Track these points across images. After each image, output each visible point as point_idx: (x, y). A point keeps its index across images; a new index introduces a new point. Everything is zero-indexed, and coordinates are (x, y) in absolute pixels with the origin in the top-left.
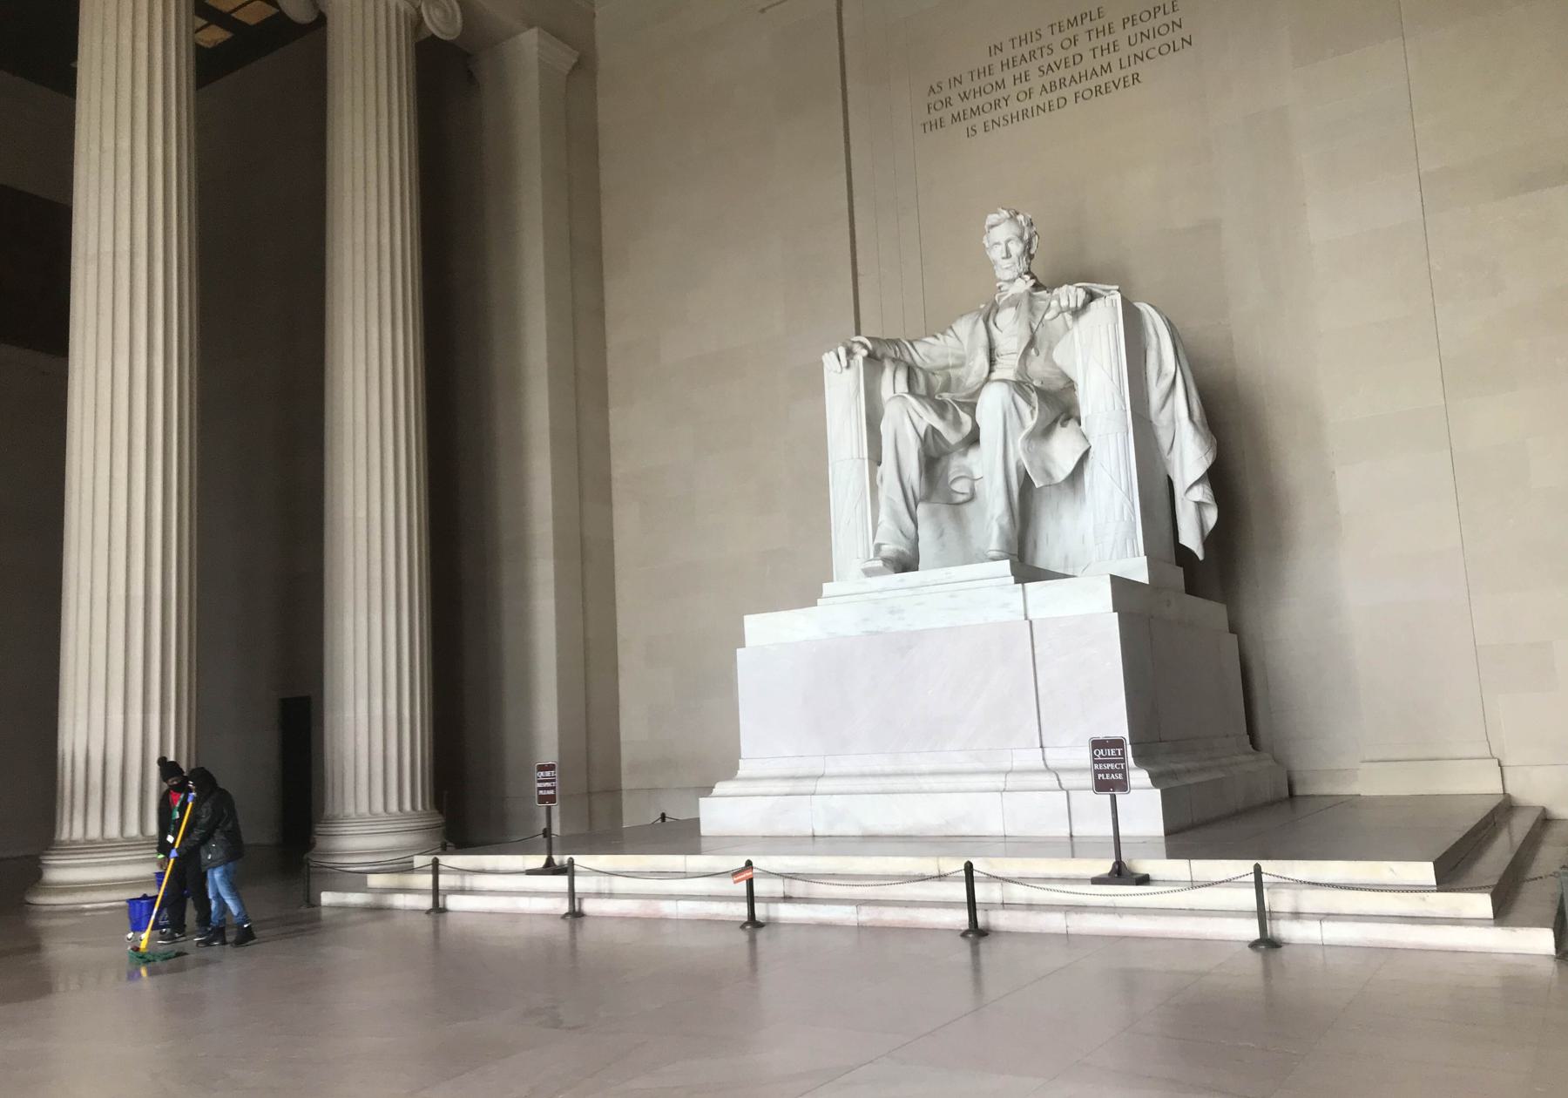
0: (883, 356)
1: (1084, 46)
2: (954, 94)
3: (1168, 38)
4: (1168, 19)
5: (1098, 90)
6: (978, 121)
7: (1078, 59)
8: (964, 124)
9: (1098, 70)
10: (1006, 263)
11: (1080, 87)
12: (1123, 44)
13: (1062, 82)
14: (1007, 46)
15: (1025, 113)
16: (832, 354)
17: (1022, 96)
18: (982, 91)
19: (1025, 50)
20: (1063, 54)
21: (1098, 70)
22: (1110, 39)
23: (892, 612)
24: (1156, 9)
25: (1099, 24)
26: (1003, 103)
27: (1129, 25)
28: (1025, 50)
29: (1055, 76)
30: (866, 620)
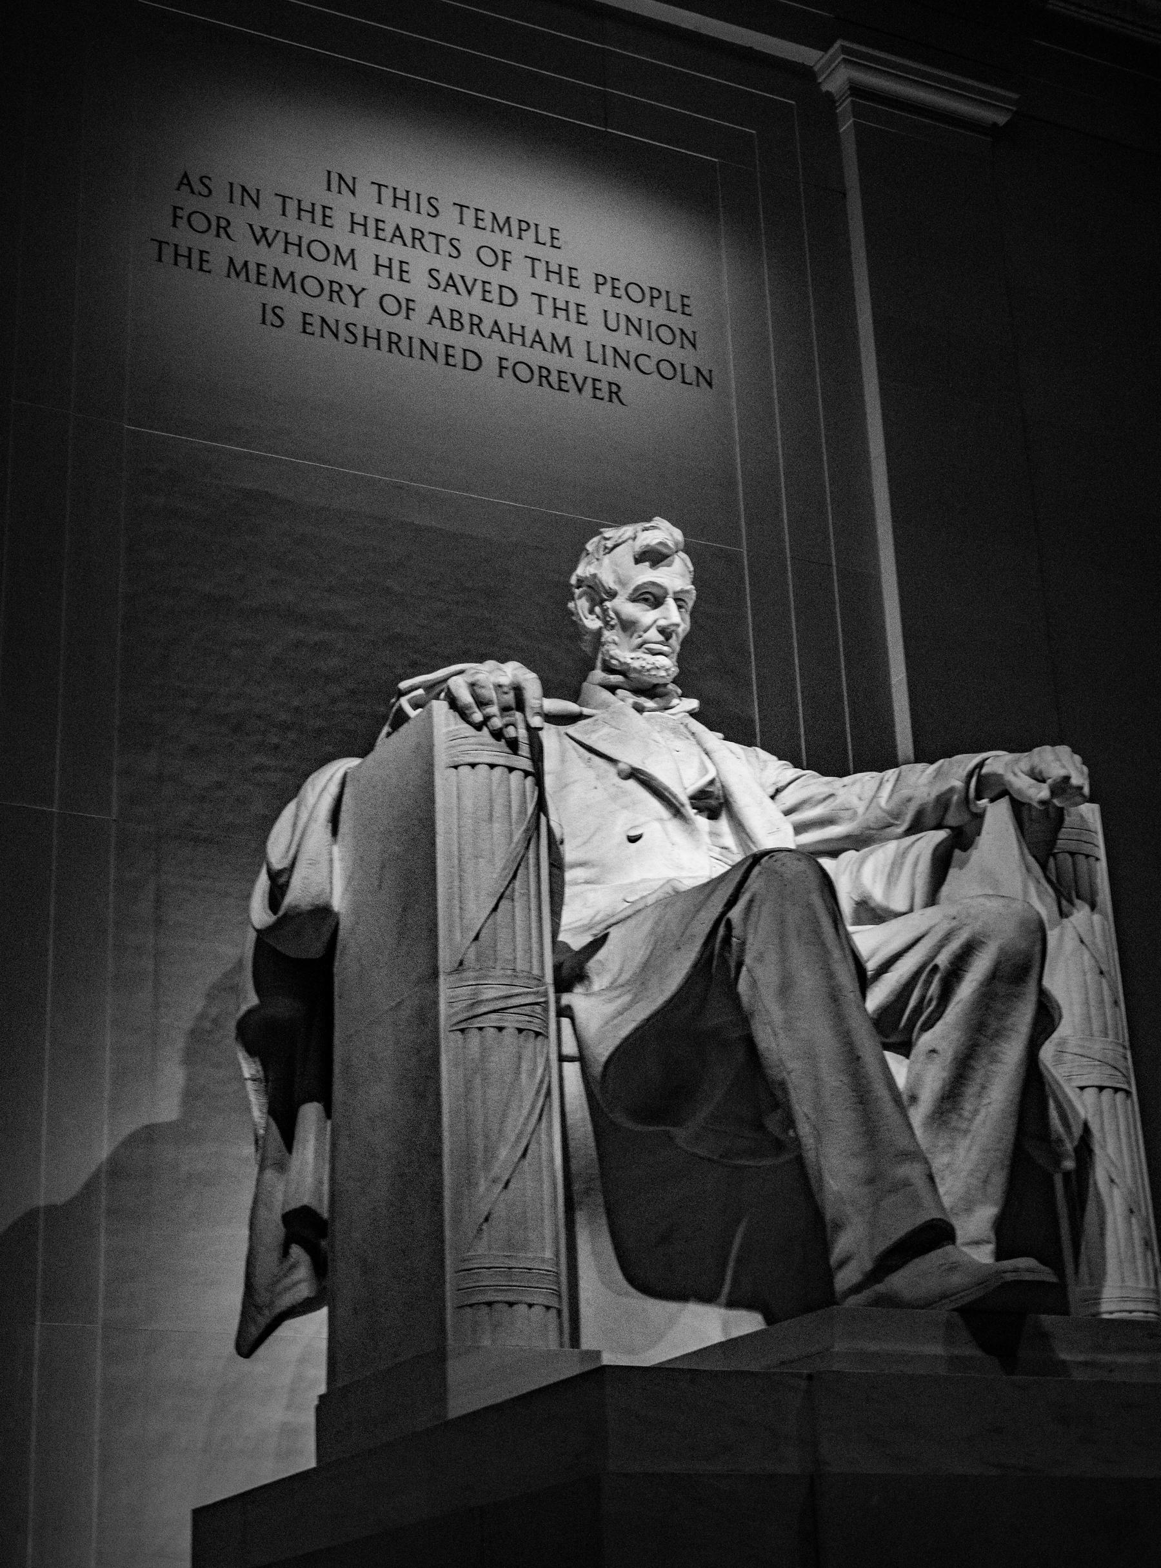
3: (675, 353)
4: (677, 321)
6: (294, 304)
7: (508, 297)
8: (254, 295)
9: (547, 341)
12: (593, 315)
13: (476, 324)
14: (365, 191)
18: (301, 247)
19: (408, 220)
20: (483, 273)
21: (547, 341)
22: (574, 297)
24: (655, 294)
25: (555, 258)
26: (346, 294)
27: (606, 290)
28: (408, 220)
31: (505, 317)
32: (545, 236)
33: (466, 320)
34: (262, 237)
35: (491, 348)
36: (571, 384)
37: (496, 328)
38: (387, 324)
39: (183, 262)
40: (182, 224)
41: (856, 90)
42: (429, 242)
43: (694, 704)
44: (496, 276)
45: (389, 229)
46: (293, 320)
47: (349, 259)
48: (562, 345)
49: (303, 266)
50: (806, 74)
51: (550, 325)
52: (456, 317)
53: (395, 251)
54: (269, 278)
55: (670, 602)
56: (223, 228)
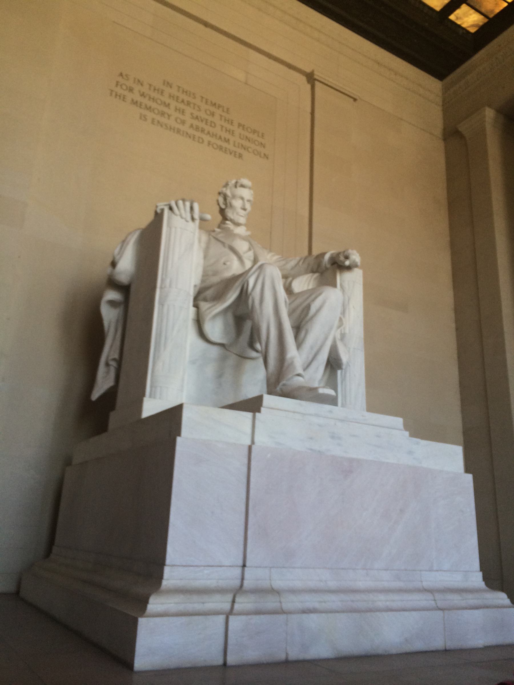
1: (216, 119)
2: (137, 88)
4: (260, 140)
5: (221, 148)
6: (150, 115)
7: (213, 125)
10: (242, 212)
11: (213, 140)
15: (179, 131)
16: (188, 204)
17: (179, 121)
19: (186, 98)
20: (206, 117)
23: (333, 437)
24: (254, 132)
26: (166, 116)
27: (241, 128)
29: (202, 125)
30: (311, 438)
31: (211, 130)
33: (200, 129)
34: (143, 95)
36: (228, 152)
37: (209, 133)
38: (177, 126)
39: (118, 97)
40: (119, 86)
42: (192, 105)
43: (249, 233)
44: (210, 119)
46: (149, 121)
47: (168, 105)
49: (154, 105)
51: (224, 135)
53: (181, 106)
54: (143, 106)
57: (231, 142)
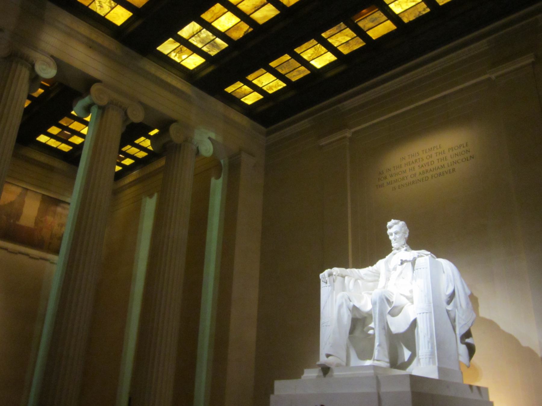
0: (346, 276)
7: (432, 163)
9: (440, 167)
13: (427, 171)
17: (412, 176)
21: (440, 167)
26: (405, 178)
32: (438, 147)
35: (429, 175)
37: (431, 170)
41: (497, 77)
42: (418, 161)
43: (405, 248)
45: (411, 163)
47: (405, 172)
48: (443, 166)
50: (489, 79)
52: (423, 172)
55: (394, 234)
56: (386, 178)
57: (446, 165)
